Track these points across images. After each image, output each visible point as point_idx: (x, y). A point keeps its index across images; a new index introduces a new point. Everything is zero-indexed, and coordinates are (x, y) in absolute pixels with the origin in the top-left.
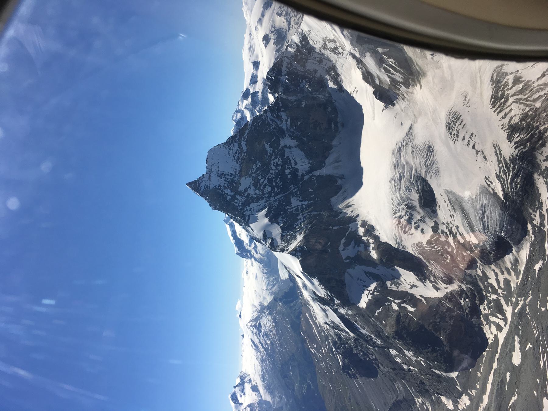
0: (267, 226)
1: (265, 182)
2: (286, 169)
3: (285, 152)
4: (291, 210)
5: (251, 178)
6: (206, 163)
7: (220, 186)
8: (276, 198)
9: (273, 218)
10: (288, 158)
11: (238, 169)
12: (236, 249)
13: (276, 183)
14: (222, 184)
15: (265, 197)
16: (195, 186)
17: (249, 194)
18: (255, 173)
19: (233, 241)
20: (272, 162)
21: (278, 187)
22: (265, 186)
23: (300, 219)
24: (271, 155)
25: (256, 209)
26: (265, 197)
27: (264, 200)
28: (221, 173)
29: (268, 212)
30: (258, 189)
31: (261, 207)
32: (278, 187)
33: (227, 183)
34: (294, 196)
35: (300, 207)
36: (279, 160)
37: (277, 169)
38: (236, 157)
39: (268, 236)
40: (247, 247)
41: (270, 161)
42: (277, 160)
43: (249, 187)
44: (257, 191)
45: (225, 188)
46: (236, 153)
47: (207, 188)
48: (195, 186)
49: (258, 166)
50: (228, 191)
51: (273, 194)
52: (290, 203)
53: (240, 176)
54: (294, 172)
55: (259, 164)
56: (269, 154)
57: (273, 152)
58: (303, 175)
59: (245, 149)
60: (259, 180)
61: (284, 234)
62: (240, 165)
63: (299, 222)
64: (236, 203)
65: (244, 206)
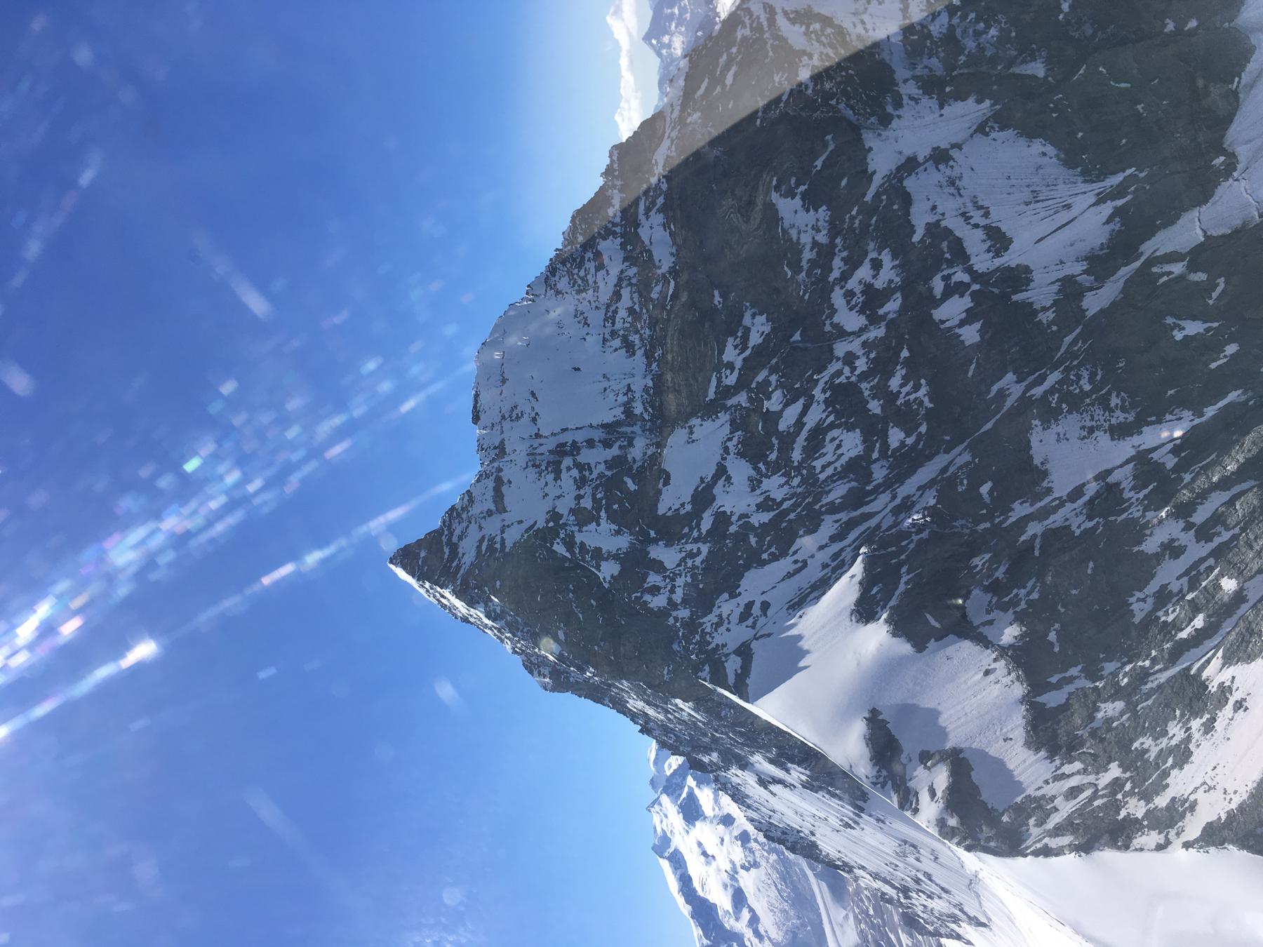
0: (887, 670)
1: (812, 419)
2: (937, 303)
3: (907, 200)
4: (1056, 520)
5: (724, 417)
6: (476, 418)
7: (554, 515)
8: (907, 488)
9: (922, 597)
10: (936, 231)
11: (640, 383)
12: (697, 932)
13: (889, 398)
14: (563, 508)
15: (833, 509)
16: (431, 557)
17: (722, 519)
18: (742, 384)
19: (686, 909)
20: (837, 298)
21: (905, 416)
22: (817, 439)
23: (1173, 550)
24: (825, 254)
25: (779, 598)
26: (833, 509)
27: (828, 526)
28: (551, 444)
29: (866, 585)
30: (774, 469)
31: (814, 573)
32: (905, 416)
33: (587, 490)
34: (1050, 416)
35: (1123, 476)
36: (877, 265)
37: (874, 320)
38: (622, 313)
39: (909, 746)
40: (730, 923)
41: (823, 290)
42: (864, 272)
43: (721, 471)
44: (775, 486)
45: (584, 518)
46: (617, 296)
47: (490, 550)
48: (431, 557)
49: (755, 339)
50: (604, 537)
51: (879, 473)
52: (1025, 477)
53: (660, 424)
54: (1000, 294)
55: (758, 328)
56: (807, 255)
57: (834, 231)
58: (1070, 291)
59: (664, 258)
60: (772, 418)
61: (1052, 699)
62: (649, 355)
63: (1169, 573)
64: (655, 590)
65: (702, 601)
